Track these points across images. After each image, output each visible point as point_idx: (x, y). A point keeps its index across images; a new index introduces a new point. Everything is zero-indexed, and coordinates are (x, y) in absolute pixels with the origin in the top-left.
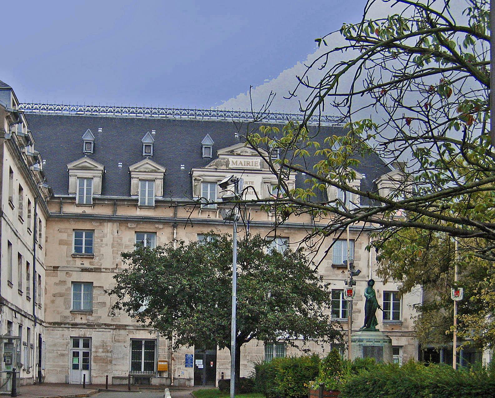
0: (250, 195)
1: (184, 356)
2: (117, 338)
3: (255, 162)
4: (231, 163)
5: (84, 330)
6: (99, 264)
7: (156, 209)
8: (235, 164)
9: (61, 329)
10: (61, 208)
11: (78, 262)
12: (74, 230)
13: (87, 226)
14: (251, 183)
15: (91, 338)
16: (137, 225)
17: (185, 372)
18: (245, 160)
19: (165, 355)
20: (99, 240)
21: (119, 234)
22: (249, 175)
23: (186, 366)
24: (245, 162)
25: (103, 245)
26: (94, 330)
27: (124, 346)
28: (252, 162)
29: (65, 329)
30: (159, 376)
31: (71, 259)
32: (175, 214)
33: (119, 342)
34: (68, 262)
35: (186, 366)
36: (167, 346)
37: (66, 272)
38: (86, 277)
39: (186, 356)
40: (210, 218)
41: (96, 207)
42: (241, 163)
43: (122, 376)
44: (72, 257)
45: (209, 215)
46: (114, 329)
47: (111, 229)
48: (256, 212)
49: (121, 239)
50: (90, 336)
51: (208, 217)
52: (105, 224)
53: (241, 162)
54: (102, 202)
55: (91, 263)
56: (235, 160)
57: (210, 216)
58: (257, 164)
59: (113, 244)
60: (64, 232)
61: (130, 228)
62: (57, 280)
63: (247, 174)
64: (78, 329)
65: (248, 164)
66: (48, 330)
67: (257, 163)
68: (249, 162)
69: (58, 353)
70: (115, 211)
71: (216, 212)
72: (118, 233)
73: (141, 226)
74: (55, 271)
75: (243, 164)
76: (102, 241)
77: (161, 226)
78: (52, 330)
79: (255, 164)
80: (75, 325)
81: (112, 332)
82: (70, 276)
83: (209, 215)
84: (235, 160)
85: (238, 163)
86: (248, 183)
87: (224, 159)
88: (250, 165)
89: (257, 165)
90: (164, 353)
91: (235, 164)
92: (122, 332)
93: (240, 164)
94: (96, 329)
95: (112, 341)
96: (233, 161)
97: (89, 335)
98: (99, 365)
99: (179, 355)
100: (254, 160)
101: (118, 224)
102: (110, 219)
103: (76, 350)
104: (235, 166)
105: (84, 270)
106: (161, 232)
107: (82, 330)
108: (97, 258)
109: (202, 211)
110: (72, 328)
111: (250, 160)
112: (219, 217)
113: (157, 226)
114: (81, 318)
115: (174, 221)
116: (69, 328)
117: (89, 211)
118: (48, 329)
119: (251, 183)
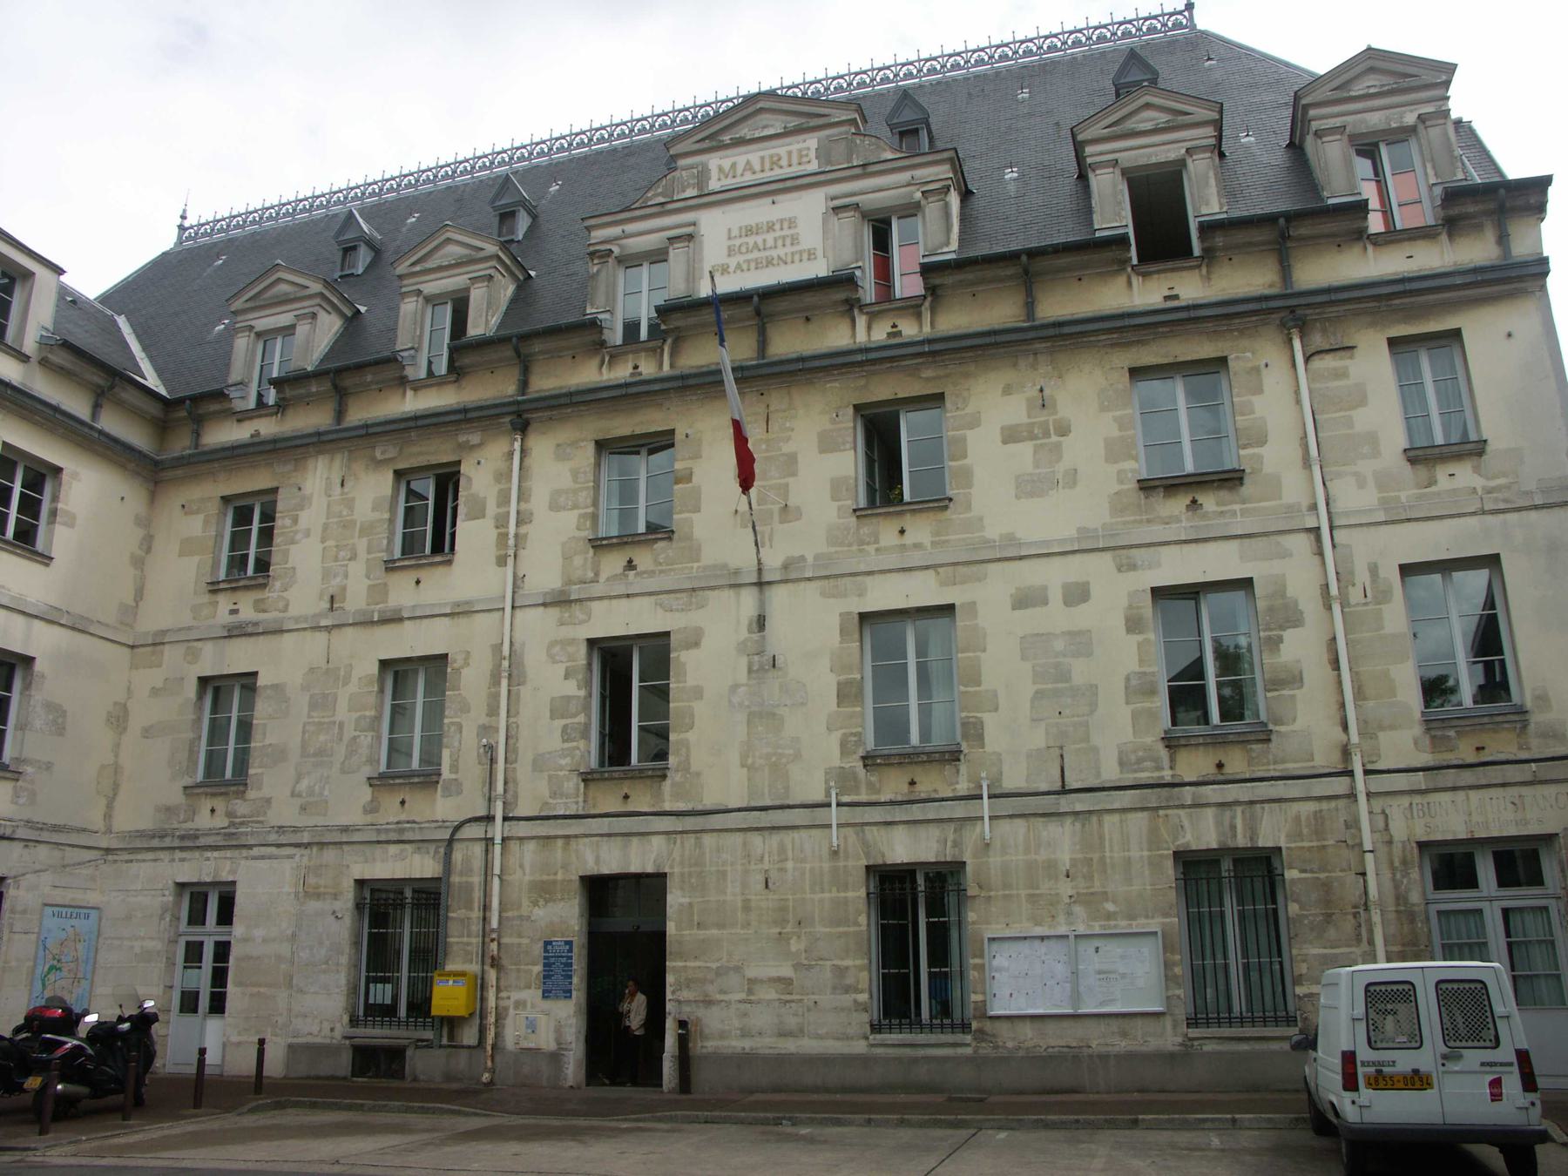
0: (783, 266)
1: (538, 949)
2: (312, 880)
3: (800, 151)
4: (714, 174)
5: (216, 854)
6: (281, 605)
7: (464, 383)
8: (731, 175)
9: (150, 855)
10: (197, 435)
11: (224, 602)
12: (226, 500)
13: (256, 480)
14: (786, 225)
15: (234, 883)
16: (401, 449)
17: (542, 1021)
18: (762, 153)
19: (469, 948)
20: (288, 522)
21: (346, 490)
22: (778, 198)
23: (546, 995)
24: (762, 158)
25: (299, 536)
26: (245, 852)
27: (334, 912)
28: (790, 153)
29: (161, 855)
30: (445, 1041)
31: (206, 598)
32: (524, 385)
33: (318, 896)
34: (196, 609)
35: (546, 995)
36: (476, 905)
37: (186, 644)
38: (238, 657)
39: (546, 951)
40: (640, 374)
41: (290, 412)
42: (749, 166)
43: (318, 1040)
44: (210, 591)
45: (636, 367)
46: (307, 846)
47: (325, 476)
48: (808, 319)
49: (350, 504)
50: (230, 878)
51: (632, 375)
52: (311, 463)
53: (748, 162)
54: (302, 391)
55: (259, 606)
56: (726, 164)
57: (640, 370)
58: (807, 155)
59: (326, 527)
60: (197, 512)
61: (381, 461)
62: (156, 677)
63: (769, 200)
64: (197, 854)
65: (776, 162)
66: (115, 861)
67: (804, 153)
68: (778, 155)
69: (132, 947)
70: (340, 414)
71: (663, 350)
72: (342, 485)
73: (415, 449)
74: (159, 648)
75: (757, 167)
76: (295, 521)
77: (475, 438)
78: (127, 862)
79: (801, 157)
80: (190, 843)
81: (297, 857)
82: (193, 656)
83: (636, 367)
84: (726, 164)
85: (740, 170)
86: (777, 227)
87: (691, 167)
88: (781, 167)
89: (805, 159)
90: (465, 939)
91: (731, 175)
92: (330, 855)
93: (744, 170)
94: (250, 847)
95: (297, 894)
96: (721, 169)
97: (229, 872)
98: (252, 995)
99: (519, 945)
100: (795, 147)
101: (346, 454)
102: (316, 443)
103: (196, 933)
104: (729, 182)
105: (237, 632)
106: (476, 455)
107: (208, 854)
108: (278, 584)
109: (611, 357)
110: (182, 849)
111: (782, 151)
112: (672, 366)
113: (462, 438)
114: (213, 811)
115: (513, 408)
116: (174, 848)
117: (267, 427)
118: (115, 857)
119: (786, 225)
